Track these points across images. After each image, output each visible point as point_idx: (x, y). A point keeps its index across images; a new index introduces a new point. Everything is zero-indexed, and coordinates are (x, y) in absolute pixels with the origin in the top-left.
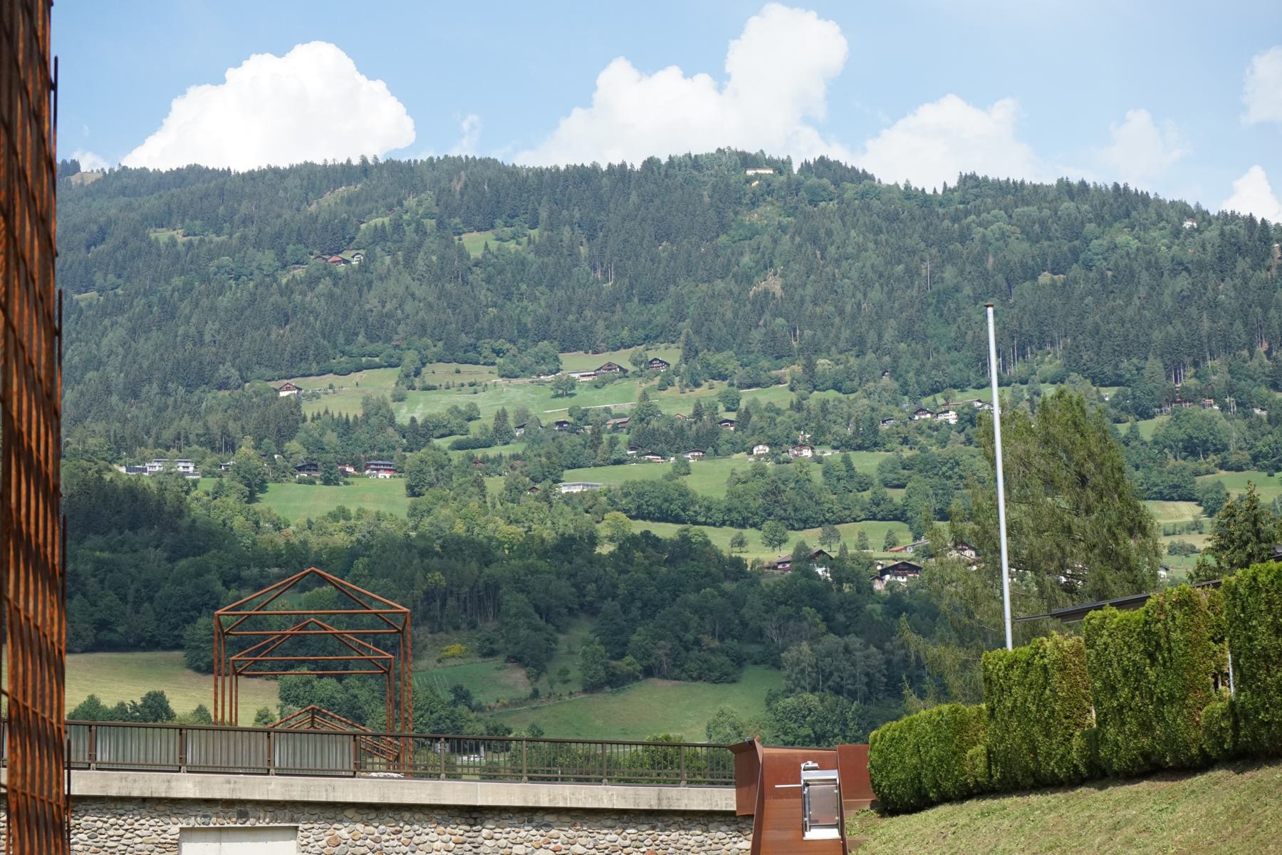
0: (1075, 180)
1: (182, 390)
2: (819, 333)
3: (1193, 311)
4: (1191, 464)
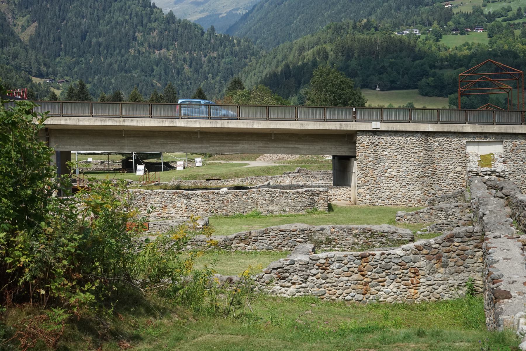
1: (414, 7)
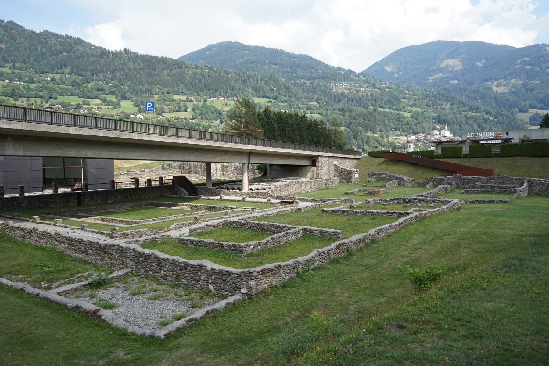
0: (69, 35)
2: (15, 58)
3: (96, 64)
4: (98, 93)
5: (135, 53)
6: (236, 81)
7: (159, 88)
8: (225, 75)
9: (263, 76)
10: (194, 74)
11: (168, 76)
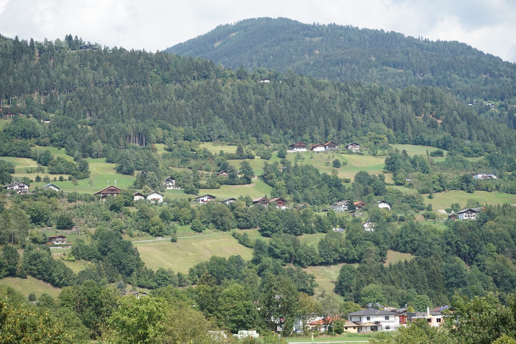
4: (23, 141)
5: (90, 46)
6: (343, 105)
7: (163, 127)
8: (315, 91)
9: (407, 92)
10: (242, 90)
11: (179, 97)
